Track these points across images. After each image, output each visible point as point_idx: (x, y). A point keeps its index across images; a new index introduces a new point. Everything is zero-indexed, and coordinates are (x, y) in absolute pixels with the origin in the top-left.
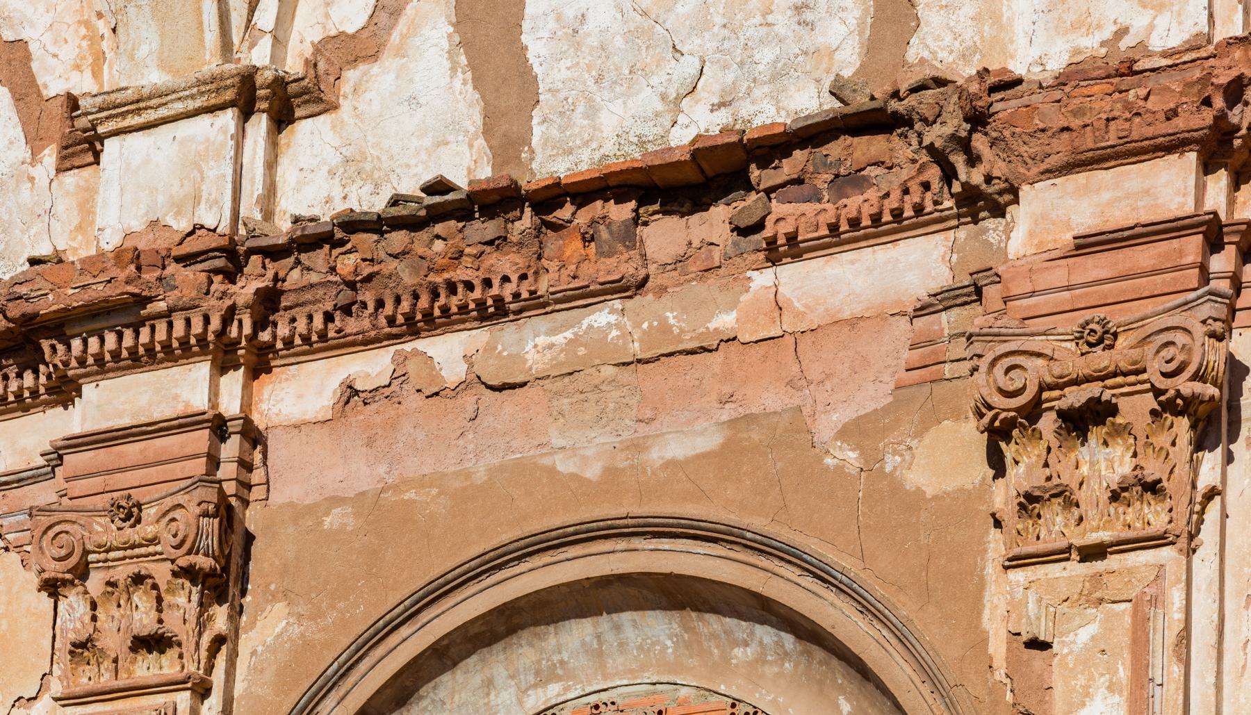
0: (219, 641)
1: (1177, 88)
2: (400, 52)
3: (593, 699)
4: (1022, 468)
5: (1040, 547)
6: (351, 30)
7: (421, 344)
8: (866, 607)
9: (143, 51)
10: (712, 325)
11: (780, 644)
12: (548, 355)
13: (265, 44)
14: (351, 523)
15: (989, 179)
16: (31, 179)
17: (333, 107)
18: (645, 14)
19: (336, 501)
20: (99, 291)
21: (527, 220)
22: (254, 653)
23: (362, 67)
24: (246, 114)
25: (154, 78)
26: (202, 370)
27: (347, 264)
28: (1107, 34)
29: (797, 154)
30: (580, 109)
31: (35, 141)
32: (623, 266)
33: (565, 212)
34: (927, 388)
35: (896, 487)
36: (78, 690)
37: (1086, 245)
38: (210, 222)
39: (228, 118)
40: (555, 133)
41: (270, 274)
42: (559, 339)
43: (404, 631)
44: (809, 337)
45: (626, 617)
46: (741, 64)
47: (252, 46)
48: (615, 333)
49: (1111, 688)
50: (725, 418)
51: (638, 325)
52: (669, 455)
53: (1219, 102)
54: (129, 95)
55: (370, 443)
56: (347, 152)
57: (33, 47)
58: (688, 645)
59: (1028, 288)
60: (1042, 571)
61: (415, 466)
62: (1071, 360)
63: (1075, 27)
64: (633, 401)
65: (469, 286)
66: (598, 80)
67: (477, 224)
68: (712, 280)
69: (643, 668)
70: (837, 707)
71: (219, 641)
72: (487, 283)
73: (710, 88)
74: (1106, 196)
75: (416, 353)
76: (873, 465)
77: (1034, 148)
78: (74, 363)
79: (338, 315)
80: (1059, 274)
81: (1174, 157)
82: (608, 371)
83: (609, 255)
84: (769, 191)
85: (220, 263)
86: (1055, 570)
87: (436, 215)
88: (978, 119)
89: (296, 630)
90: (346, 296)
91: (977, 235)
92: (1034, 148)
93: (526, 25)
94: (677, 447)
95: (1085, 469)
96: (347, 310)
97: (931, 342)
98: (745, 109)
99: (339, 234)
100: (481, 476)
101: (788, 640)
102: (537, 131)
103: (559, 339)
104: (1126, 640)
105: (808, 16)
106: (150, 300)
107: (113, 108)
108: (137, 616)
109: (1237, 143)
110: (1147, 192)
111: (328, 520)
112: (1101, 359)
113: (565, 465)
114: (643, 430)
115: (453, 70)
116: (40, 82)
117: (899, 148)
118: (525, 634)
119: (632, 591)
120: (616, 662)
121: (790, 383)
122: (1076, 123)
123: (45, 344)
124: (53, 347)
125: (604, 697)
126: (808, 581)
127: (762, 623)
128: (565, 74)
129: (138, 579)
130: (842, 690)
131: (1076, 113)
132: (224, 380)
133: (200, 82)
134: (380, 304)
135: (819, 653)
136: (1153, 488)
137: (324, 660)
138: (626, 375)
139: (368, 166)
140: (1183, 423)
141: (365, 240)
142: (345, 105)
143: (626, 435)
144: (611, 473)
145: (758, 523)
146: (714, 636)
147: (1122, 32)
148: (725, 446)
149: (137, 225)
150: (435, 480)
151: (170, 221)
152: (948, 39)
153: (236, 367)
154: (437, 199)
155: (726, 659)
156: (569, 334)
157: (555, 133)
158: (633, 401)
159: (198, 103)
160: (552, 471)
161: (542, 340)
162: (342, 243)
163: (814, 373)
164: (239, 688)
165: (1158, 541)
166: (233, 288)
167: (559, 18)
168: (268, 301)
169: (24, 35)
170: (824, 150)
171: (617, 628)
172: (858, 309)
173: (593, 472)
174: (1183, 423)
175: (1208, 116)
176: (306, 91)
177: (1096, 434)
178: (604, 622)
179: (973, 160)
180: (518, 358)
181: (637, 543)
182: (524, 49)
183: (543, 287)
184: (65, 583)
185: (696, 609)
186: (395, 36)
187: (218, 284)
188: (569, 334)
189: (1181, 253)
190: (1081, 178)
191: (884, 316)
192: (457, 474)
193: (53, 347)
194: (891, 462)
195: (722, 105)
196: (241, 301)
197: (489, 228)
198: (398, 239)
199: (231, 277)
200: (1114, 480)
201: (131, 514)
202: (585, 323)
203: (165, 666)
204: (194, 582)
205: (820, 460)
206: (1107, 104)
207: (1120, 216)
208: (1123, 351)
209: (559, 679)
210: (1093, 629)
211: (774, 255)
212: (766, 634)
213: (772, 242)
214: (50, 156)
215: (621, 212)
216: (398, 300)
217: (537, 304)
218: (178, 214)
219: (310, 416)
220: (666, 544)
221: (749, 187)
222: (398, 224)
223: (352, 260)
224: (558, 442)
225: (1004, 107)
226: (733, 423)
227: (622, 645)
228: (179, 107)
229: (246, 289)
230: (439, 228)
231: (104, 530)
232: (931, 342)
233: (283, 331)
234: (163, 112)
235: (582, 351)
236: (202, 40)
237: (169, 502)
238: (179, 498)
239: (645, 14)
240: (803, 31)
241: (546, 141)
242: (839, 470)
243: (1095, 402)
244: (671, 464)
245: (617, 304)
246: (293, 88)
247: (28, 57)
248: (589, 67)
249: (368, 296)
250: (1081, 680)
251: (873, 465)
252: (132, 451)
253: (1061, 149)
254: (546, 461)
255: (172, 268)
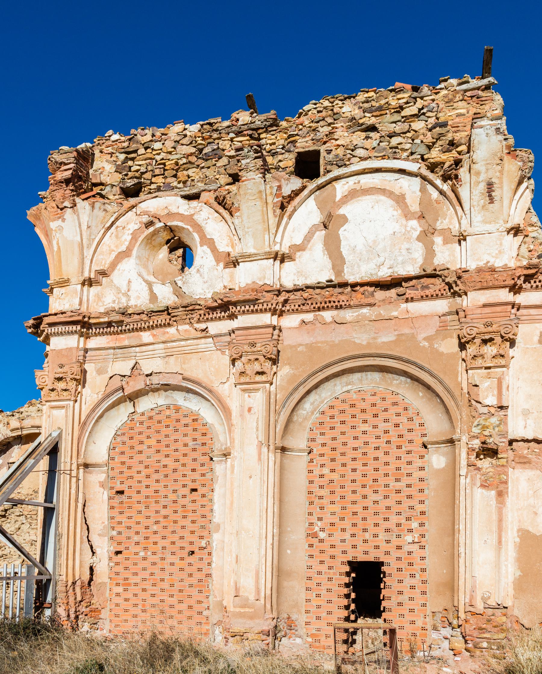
0: (275, 373)
1: (505, 275)
2: (310, 250)
3: (359, 389)
4: (471, 350)
5: (477, 366)
6: (298, 244)
7: (320, 313)
8: (431, 375)
9: (250, 244)
10: (392, 314)
11: (406, 381)
12: (352, 318)
13: (278, 245)
14: (305, 350)
15: (460, 290)
16: (217, 269)
17: (295, 260)
18: (371, 247)
19: (301, 345)
20: (247, 297)
21: (349, 289)
22: (281, 376)
23: (301, 252)
24: (275, 260)
25: (252, 251)
26: (269, 315)
27: (305, 295)
28: (485, 262)
29: (414, 281)
30: (356, 266)
31: (218, 261)
32: (370, 300)
33: (358, 288)
34: (444, 331)
35: (437, 351)
36: (241, 382)
37: (485, 306)
38: (268, 283)
39: (272, 260)
40: (350, 270)
41: (287, 296)
42: (355, 314)
43: (319, 373)
44: (415, 319)
45: (369, 373)
46: (394, 260)
47: (275, 245)
48: (368, 314)
49: (493, 395)
50: (396, 334)
51: (374, 313)
52: (383, 340)
53: (516, 279)
54: (247, 254)
55: (308, 333)
56: (298, 270)
57: (215, 240)
58: (383, 380)
59: (472, 313)
60: (476, 371)
61: (319, 339)
62: (483, 330)
63: (477, 260)
64: (373, 329)
65: (334, 302)
66: (360, 260)
67: (337, 289)
68: (391, 304)
69: (371, 383)
70: (419, 394)
71: (275, 373)
72: (339, 302)
73: (388, 263)
74: (488, 296)
75: (319, 315)
76: (431, 346)
77: (472, 284)
78: (237, 311)
79: (301, 306)
80: (479, 311)
81: (504, 289)
82: (367, 322)
83: (368, 298)
84: (406, 288)
85: (277, 293)
86: (479, 371)
87: (328, 286)
88: (459, 278)
89: (292, 372)
90: (304, 302)
91: (454, 301)
92: (472, 284)
93: (342, 247)
94: (385, 339)
95: (486, 351)
96: (303, 305)
97: (445, 322)
98: (396, 269)
99: (305, 289)
100: (337, 342)
101: (409, 380)
102: (346, 270)
103: (355, 314)
104: (496, 386)
105: (410, 251)
106: (259, 299)
107: (243, 256)
108: (255, 367)
109: (517, 287)
110: (497, 296)
111: (299, 349)
112: (490, 329)
113: (357, 341)
114: (376, 335)
115: (324, 254)
116: (218, 248)
117: (438, 281)
118: (345, 375)
119: (373, 368)
120: (365, 382)
121: (411, 328)
122: (482, 280)
123: (231, 307)
124: (232, 308)
125: (361, 389)
126: (417, 369)
127: (403, 376)
128: (352, 258)
129: (257, 359)
130: (421, 391)
131: (482, 278)
132: (273, 317)
133: (265, 253)
134: (312, 304)
135: (416, 383)
136: (502, 356)
137: (301, 379)
138: (371, 323)
139: (304, 274)
140: (509, 343)
141: (311, 290)
142: (297, 260)
143: (372, 336)
144: (369, 344)
145: (405, 356)
146: (389, 378)
147: (488, 262)
148: (396, 340)
149: (249, 282)
150: (325, 342)
151: (258, 282)
152: (443, 259)
153: (276, 315)
154: (329, 283)
155: (391, 383)
156: (357, 314)
157: (350, 270)
158: (373, 329)
159: (264, 257)
160: (354, 342)
161: (350, 314)
162: (305, 291)
163: (417, 326)
164: (278, 383)
165: (503, 366)
166: (278, 298)
167: (350, 246)
168: (286, 301)
169: (213, 237)
170: (420, 280)
171: (366, 375)
172: (427, 314)
173: (364, 343)
174: (509, 343)
175: (513, 282)
176: (289, 256)
177: (489, 344)
178: (364, 374)
179: (457, 285)
180: (345, 318)
181: (375, 358)
182: (341, 252)
183: (352, 303)
184: (237, 359)
185: (387, 372)
186: (309, 246)
187: (275, 297)
188: (357, 314)
189: (507, 309)
190: (482, 291)
191: (432, 316)
192: (331, 341)
193: (232, 308)
194: (436, 346)
195: (390, 268)
196: (280, 301)
197: (340, 290)
198: (318, 291)
199: (278, 296)
200: (493, 354)
201: (253, 345)
202: (361, 311)
203: (263, 378)
204: (270, 361)
205: (419, 344)
206: (489, 277)
207: (492, 300)
208: (495, 328)
209: (351, 385)
210: (488, 383)
211: (407, 301)
212: (403, 379)
213: (407, 299)
214: (222, 265)
215: (371, 289)
216: (316, 304)
217: (350, 306)
218: (260, 280)
219: (293, 326)
220: (383, 359)
221: (401, 286)
222: (318, 288)
223: (307, 294)
224: (355, 336)
225: (465, 276)
226: (398, 335)
227: (367, 379)
228: (260, 257)
229: (281, 299)
230: (328, 289)
231: (247, 348)
232: (445, 322)
233: (288, 308)
234: (255, 258)
235: (360, 317)
236: (264, 243)
237: (264, 343)
238: (267, 343)
239: (371, 247)
240: (409, 254)
241: (348, 272)
242: (424, 346)
243: (491, 338)
244: (383, 342)
245: (369, 308)
246: (285, 256)
247: (214, 242)
248: (358, 257)
249: (310, 302)
250: (486, 394)
251: (431, 346)
252: (253, 331)
253: (479, 285)
254: (353, 340)
255: (264, 293)
